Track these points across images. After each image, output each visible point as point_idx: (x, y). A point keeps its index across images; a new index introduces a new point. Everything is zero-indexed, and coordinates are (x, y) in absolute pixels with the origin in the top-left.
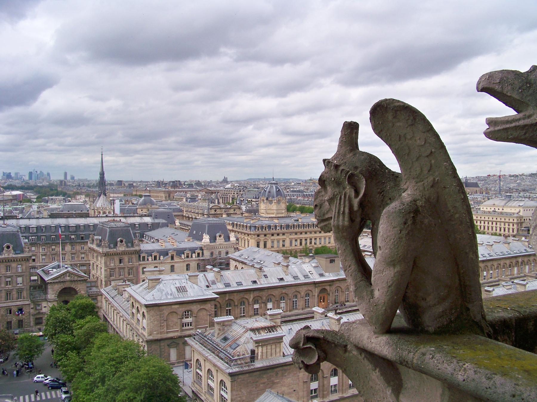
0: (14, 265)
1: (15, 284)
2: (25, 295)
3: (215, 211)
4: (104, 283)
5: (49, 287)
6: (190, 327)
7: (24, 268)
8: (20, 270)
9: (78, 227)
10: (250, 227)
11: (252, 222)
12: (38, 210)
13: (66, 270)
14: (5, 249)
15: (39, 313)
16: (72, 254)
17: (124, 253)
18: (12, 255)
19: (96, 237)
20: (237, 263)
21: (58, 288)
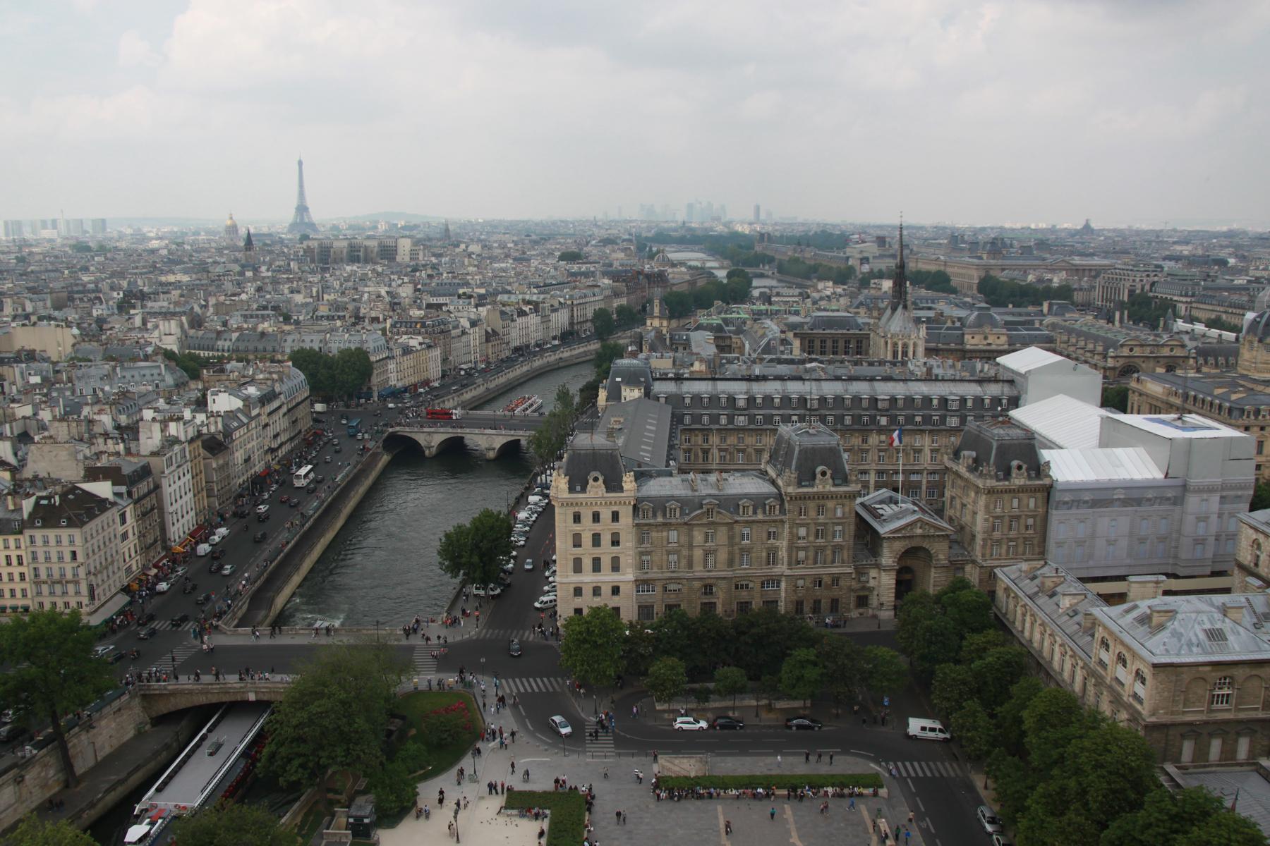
0: (830, 504)
1: (830, 538)
2: (845, 557)
3: (1131, 350)
4: (979, 541)
5: (885, 545)
6: (1225, 706)
7: (847, 509)
8: (839, 513)
9: (893, 400)
10: (1230, 410)
11: (1234, 397)
12: (783, 336)
13: (915, 517)
14: (819, 476)
15: (864, 588)
16: (880, 450)
17: (1022, 489)
18: (829, 488)
19: (966, 453)
20: (1261, 538)
21: (900, 546)
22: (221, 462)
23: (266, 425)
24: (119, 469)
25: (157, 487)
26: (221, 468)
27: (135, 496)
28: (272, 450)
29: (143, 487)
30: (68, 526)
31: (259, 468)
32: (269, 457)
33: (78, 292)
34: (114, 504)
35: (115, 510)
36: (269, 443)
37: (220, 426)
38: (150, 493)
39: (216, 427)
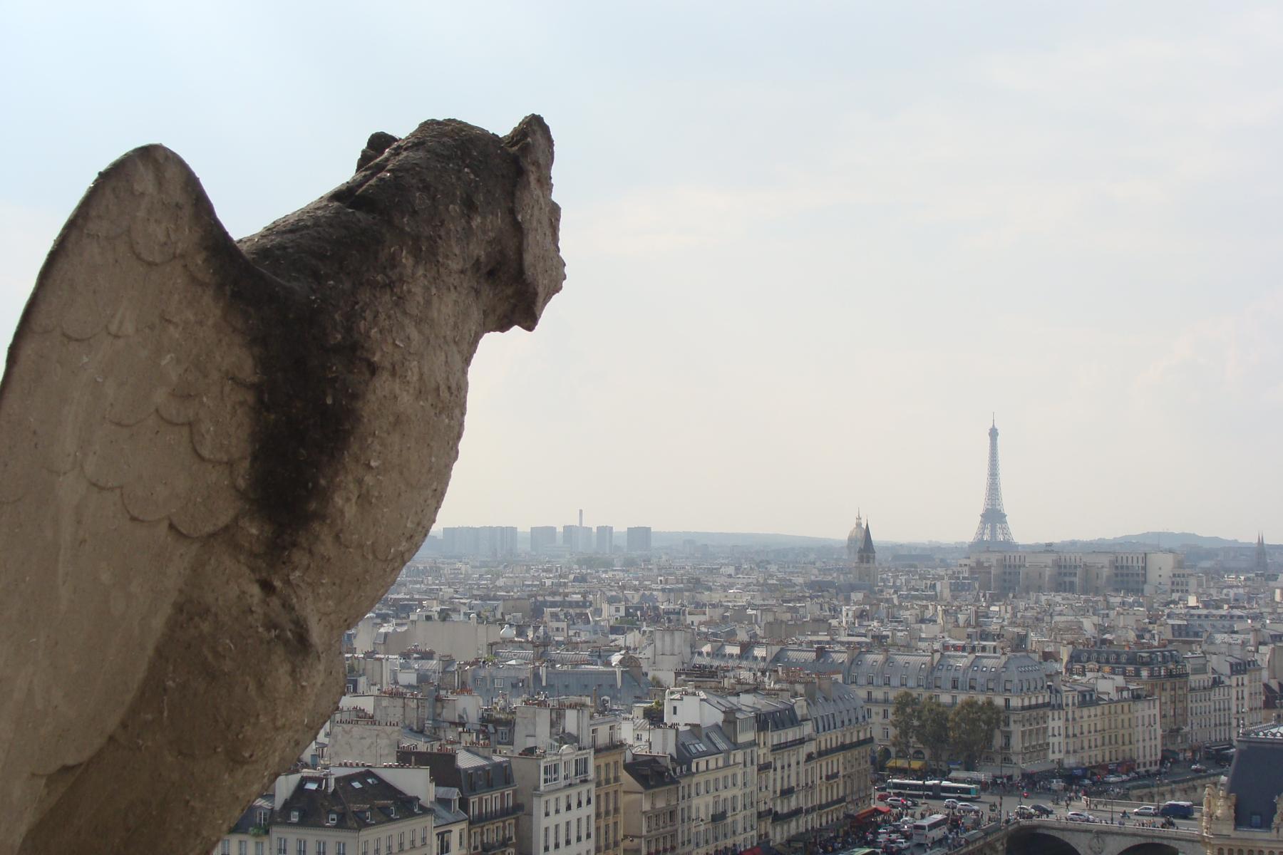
22: (661, 804)
23: (764, 768)
24: (452, 757)
25: (518, 811)
26: (653, 816)
27: (474, 810)
28: (778, 818)
29: (492, 800)
30: (341, 825)
31: (744, 838)
32: (766, 826)
33: (554, 604)
34: (425, 811)
35: (429, 821)
36: (768, 800)
37: (671, 749)
38: (504, 813)
39: (659, 744)
